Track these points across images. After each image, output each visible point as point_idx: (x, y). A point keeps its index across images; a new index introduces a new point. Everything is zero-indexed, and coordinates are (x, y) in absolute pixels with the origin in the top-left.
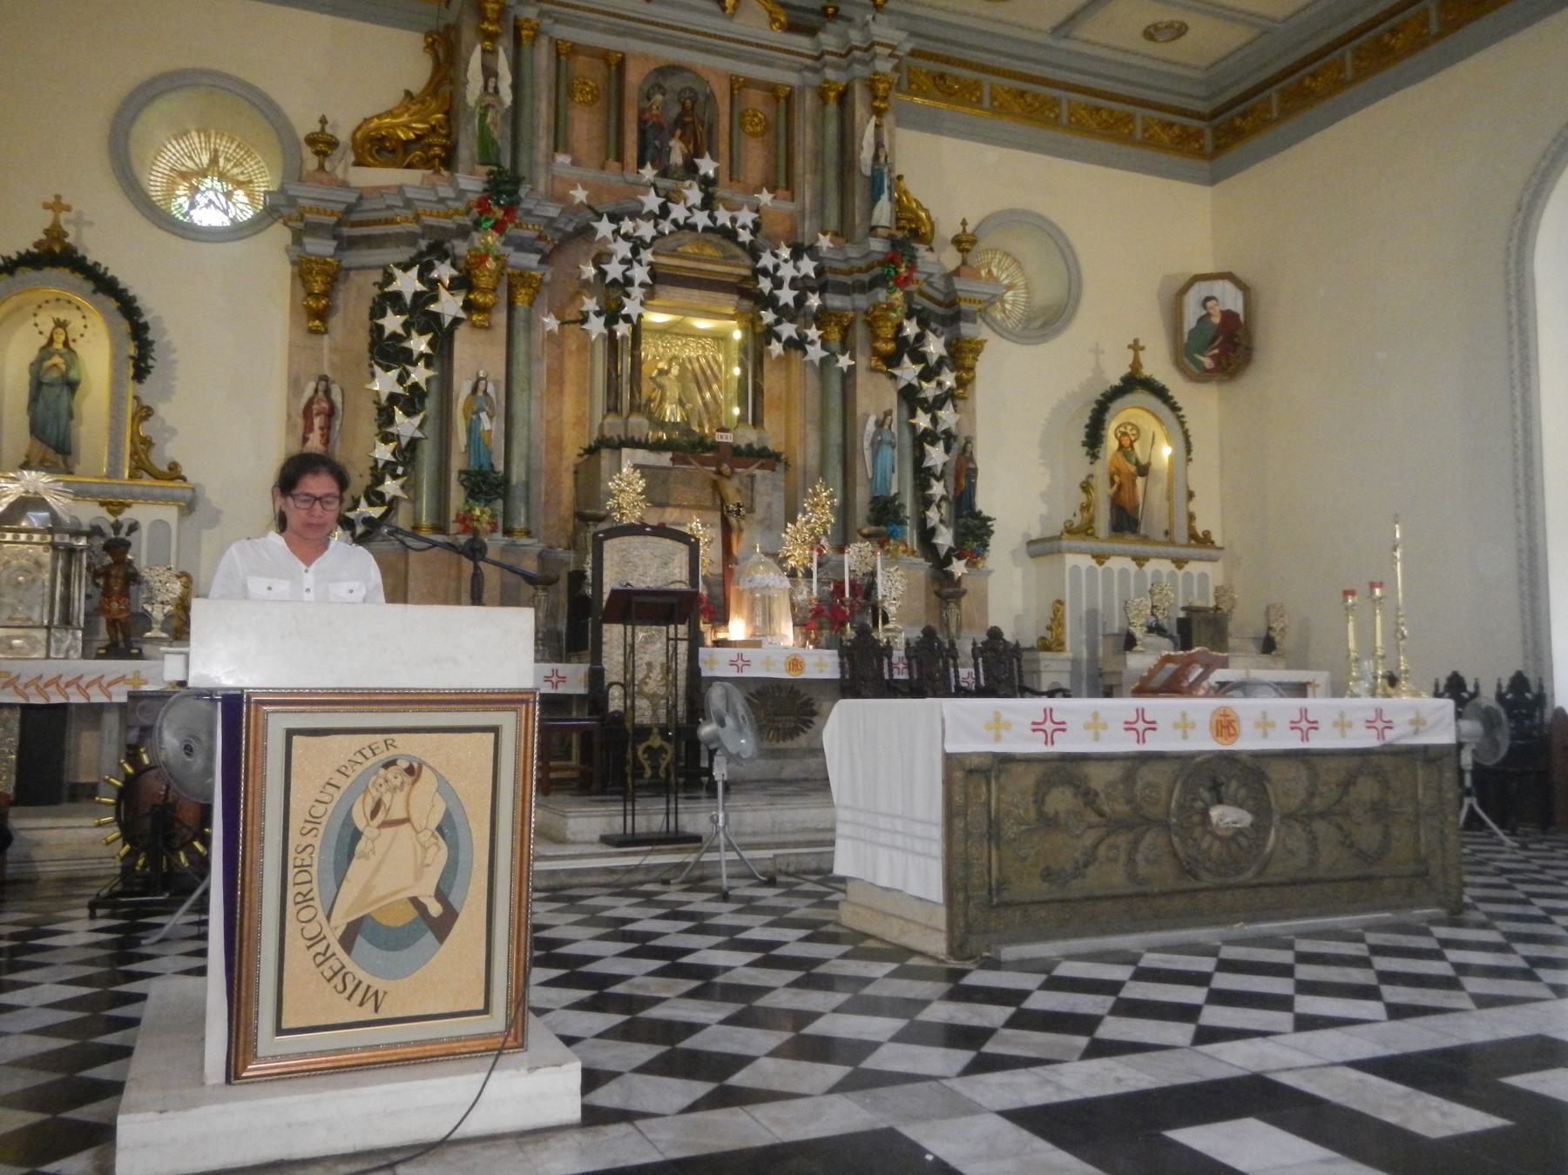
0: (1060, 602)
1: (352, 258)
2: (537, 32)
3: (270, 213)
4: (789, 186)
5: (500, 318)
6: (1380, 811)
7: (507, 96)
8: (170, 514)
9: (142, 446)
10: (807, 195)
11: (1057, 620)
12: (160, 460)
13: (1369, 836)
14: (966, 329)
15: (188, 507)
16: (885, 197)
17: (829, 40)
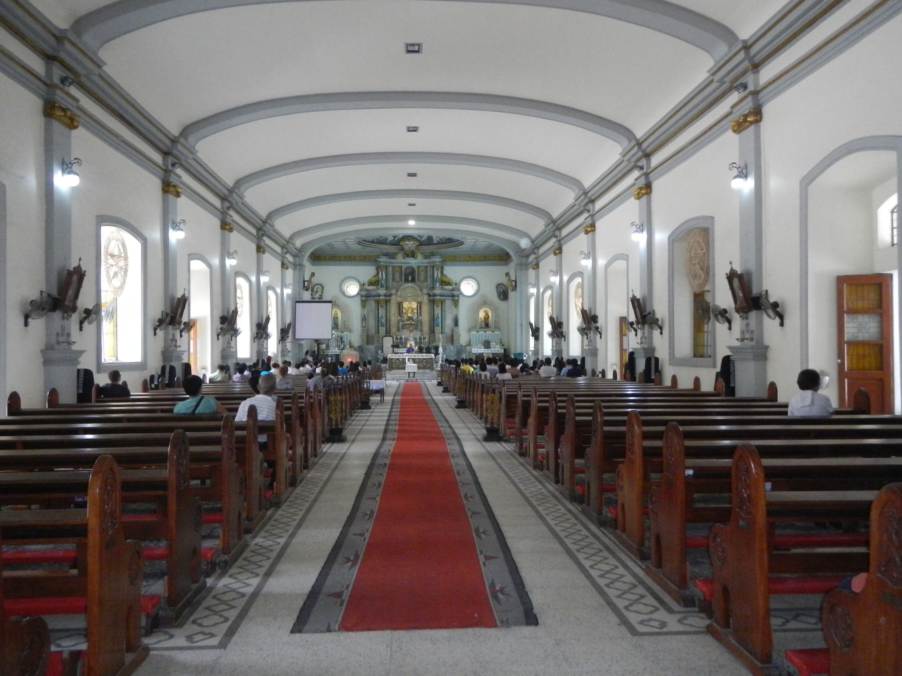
0: (470, 339)
1: (368, 298)
2: (389, 266)
3: (358, 294)
4: (427, 280)
5: (385, 307)
6: (426, 362)
7: (384, 278)
8: (348, 333)
9: (345, 325)
10: (429, 283)
11: (470, 342)
12: (347, 327)
13: (425, 364)
14: (456, 298)
15: (350, 331)
16: (438, 284)
17: (430, 260)
